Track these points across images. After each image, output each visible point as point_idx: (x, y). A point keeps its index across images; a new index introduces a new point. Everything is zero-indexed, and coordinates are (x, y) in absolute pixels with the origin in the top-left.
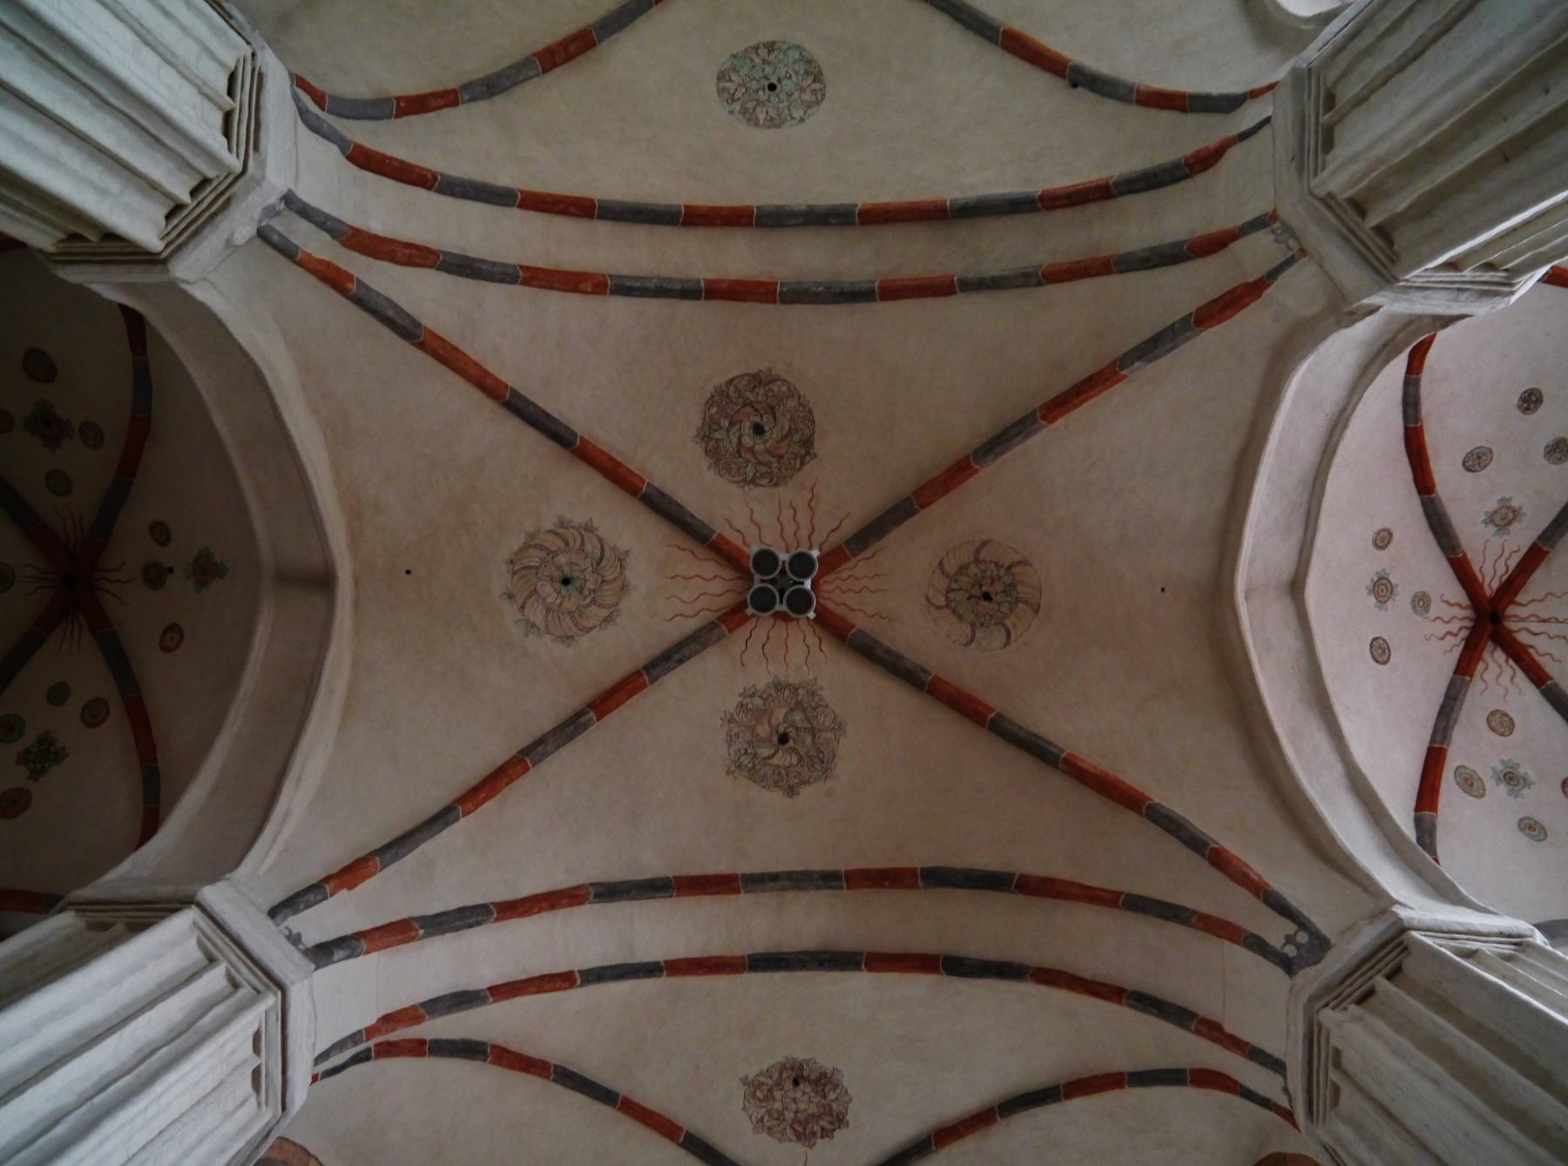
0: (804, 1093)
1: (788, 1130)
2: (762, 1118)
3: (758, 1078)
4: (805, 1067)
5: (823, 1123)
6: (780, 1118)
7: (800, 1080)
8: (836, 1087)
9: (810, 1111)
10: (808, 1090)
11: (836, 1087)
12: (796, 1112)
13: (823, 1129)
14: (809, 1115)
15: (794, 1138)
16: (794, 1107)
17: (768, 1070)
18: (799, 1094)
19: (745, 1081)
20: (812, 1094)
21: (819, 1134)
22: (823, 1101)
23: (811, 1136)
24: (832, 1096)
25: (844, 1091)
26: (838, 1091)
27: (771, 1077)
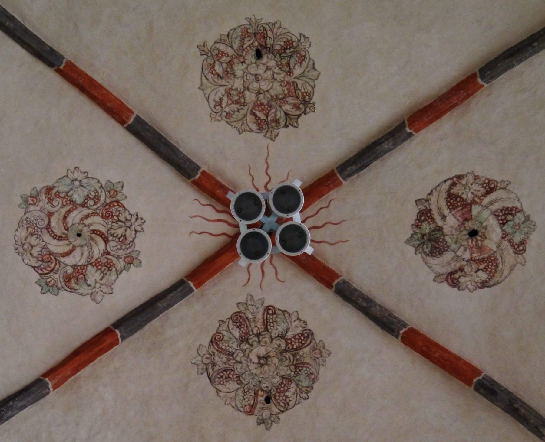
0: (267, 69)
1: (250, 118)
2: (221, 100)
3: (218, 45)
4: (269, 33)
5: (287, 108)
6: (240, 102)
7: (263, 52)
8: (303, 58)
9: (273, 92)
10: (272, 63)
11: (303, 58)
12: (259, 93)
13: (286, 114)
14: (272, 97)
15: (254, 127)
16: (255, 86)
17: (228, 36)
18: (261, 71)
19: (203, 49)
20: (277, 70)
21: (282, 122)
22: (288, 78)
23: (274, 124)
24: (298, 71)
25: (311, 63)
26: (305, 64)
27: (231, 47)
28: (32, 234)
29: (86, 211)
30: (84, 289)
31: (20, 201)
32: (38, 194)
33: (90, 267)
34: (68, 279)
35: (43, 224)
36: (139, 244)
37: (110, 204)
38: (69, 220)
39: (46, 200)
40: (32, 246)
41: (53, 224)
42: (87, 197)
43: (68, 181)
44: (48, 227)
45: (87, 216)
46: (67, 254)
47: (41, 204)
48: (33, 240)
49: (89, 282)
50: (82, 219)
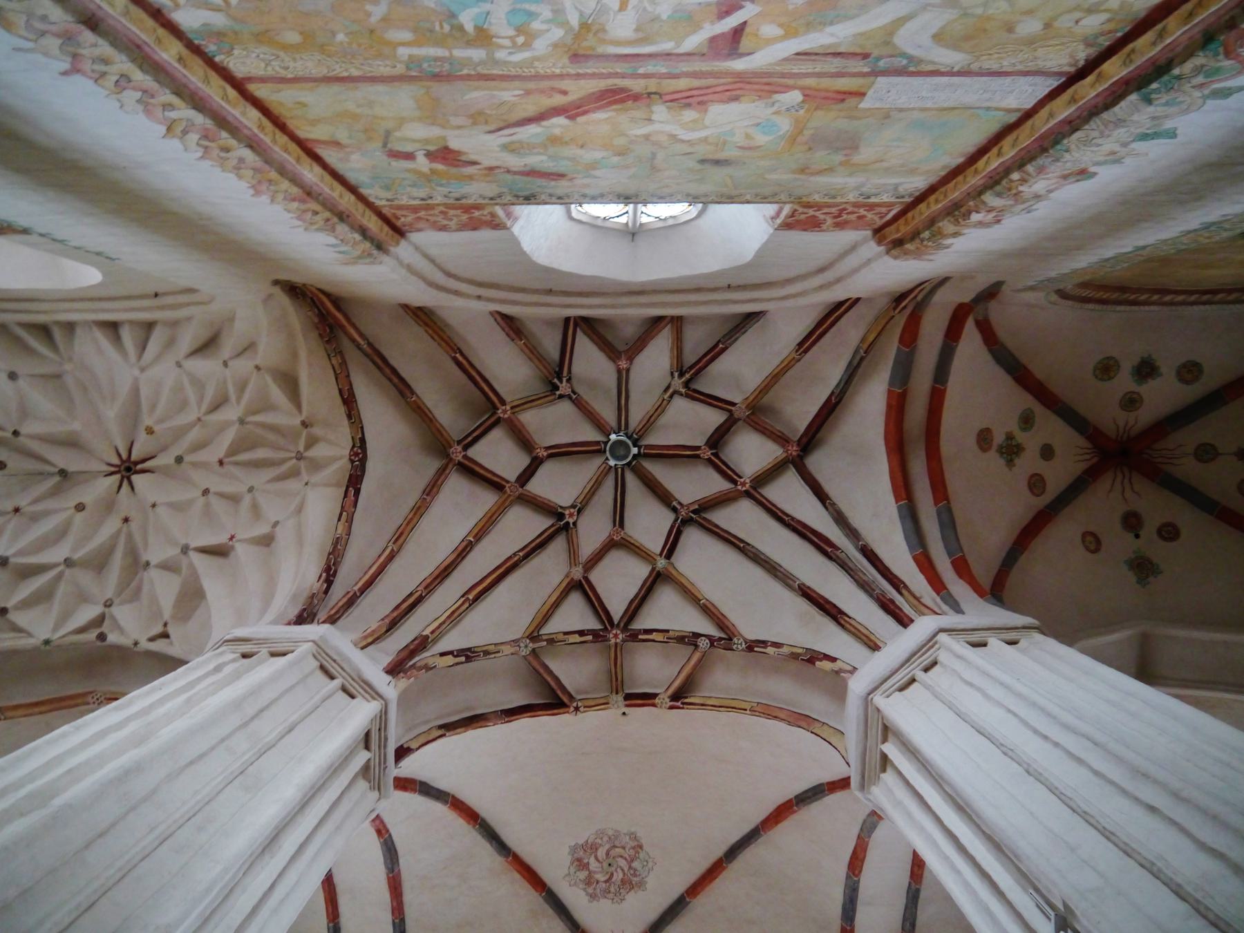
28: (610, 838)
29: (626, 869)
30: (572, 870)
31: (633, 830)
32: (638, 841)
33: (587, 872)
34: (579, 860)
35: (617, 843)
36: (603, 901)
37: (631, 883)
38: (620, 859)
39: (633, 845)
40: (602, 838)
41: (617, 850)
42: (635, 870)
43: (647, 858)
44: (615, 847)
45: (623, 870)
46: (596, 858)
47: (631, 842)
48: (605, 839)
49: (578, 873)
50: (620, 867)
